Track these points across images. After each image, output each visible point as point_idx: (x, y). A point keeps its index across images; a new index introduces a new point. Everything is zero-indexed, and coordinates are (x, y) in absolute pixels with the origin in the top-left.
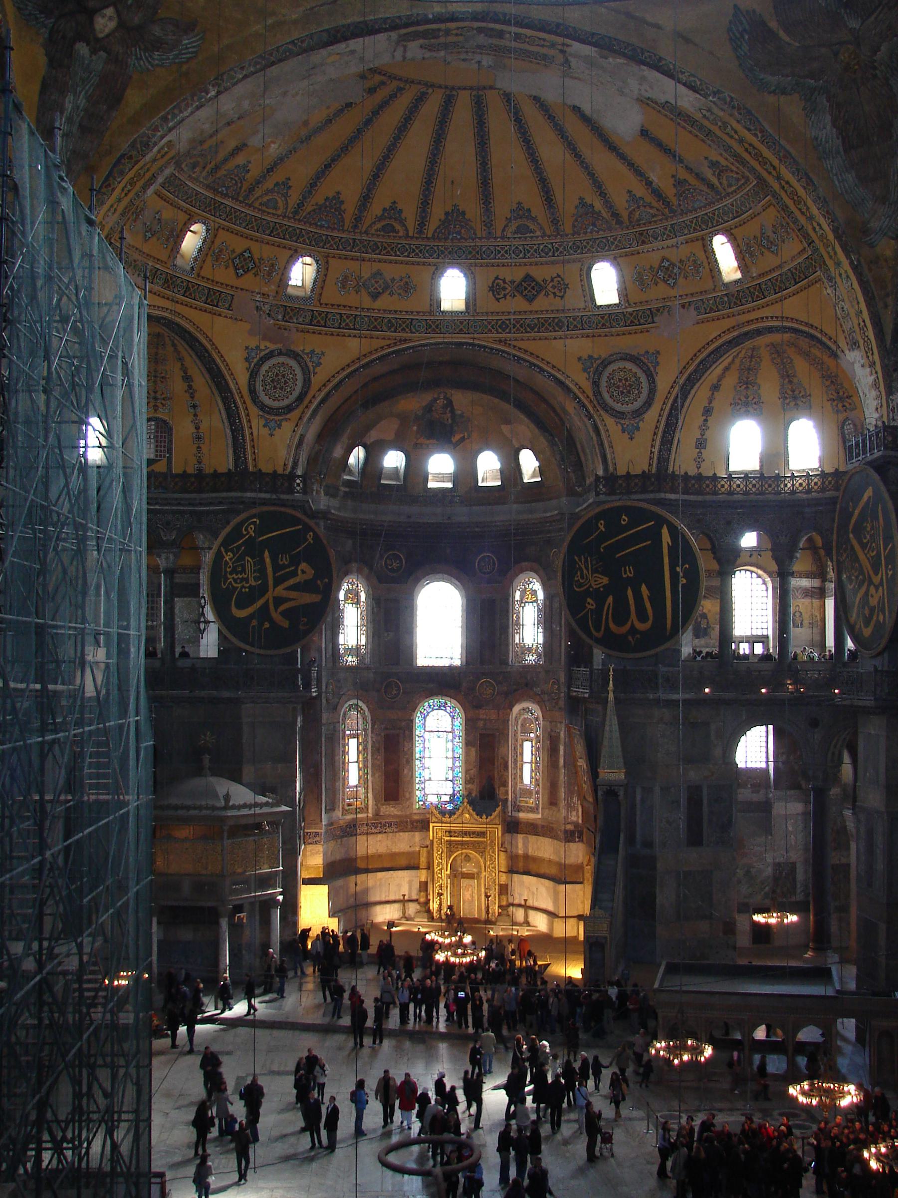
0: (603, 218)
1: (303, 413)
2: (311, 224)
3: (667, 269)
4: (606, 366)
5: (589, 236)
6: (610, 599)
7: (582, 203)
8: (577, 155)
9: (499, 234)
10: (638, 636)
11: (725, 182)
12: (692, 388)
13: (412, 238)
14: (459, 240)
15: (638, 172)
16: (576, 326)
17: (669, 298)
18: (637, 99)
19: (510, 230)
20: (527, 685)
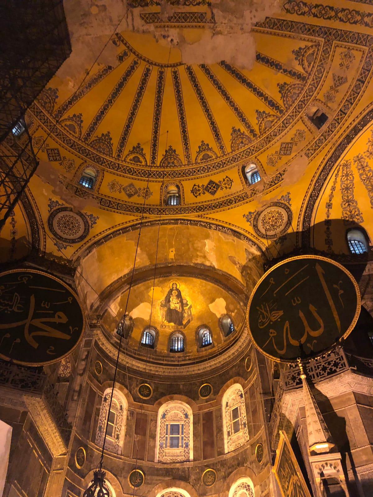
0: (246, 136)
1: (82, 246)
2: (94, 149)
3: (285, 147)
4: (259, 215)
6: (287, 324)
7: (234, 131)
8: (228, 98)
9: (194, 162)
10: (315, 341)
11: (306, 64)
12: (314, 203)
14: (173, 167)
15: (260, 94)
16: (239, 200)
17: (289, 161)
18: (253, 30)
19: (199, 159)
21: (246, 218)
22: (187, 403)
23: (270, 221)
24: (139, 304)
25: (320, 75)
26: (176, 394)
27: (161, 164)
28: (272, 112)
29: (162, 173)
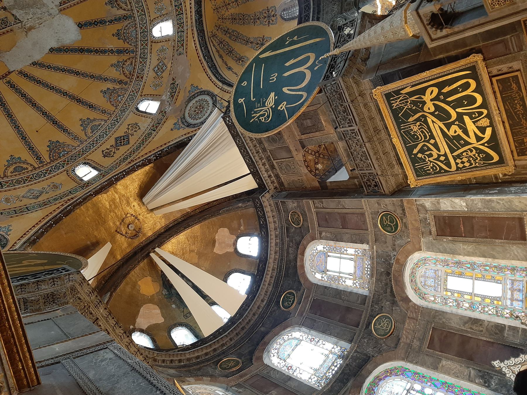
0: (118, 89)
3: (159, 69)
4: (184, 118)
5: (123, 102)
6: (285, 90)
8: (77, 73)
9: (86, 138)
13: (39, 167)
15: (104, 52)
20: (388, 274)
21: (175, 129)
22: (284, 329)
23: (197, 111)
24: (139, 311)
25: (140, 4)
26: (263, 338)
27: (52, 158)
28: (125, 57)
29: (58, 165)
